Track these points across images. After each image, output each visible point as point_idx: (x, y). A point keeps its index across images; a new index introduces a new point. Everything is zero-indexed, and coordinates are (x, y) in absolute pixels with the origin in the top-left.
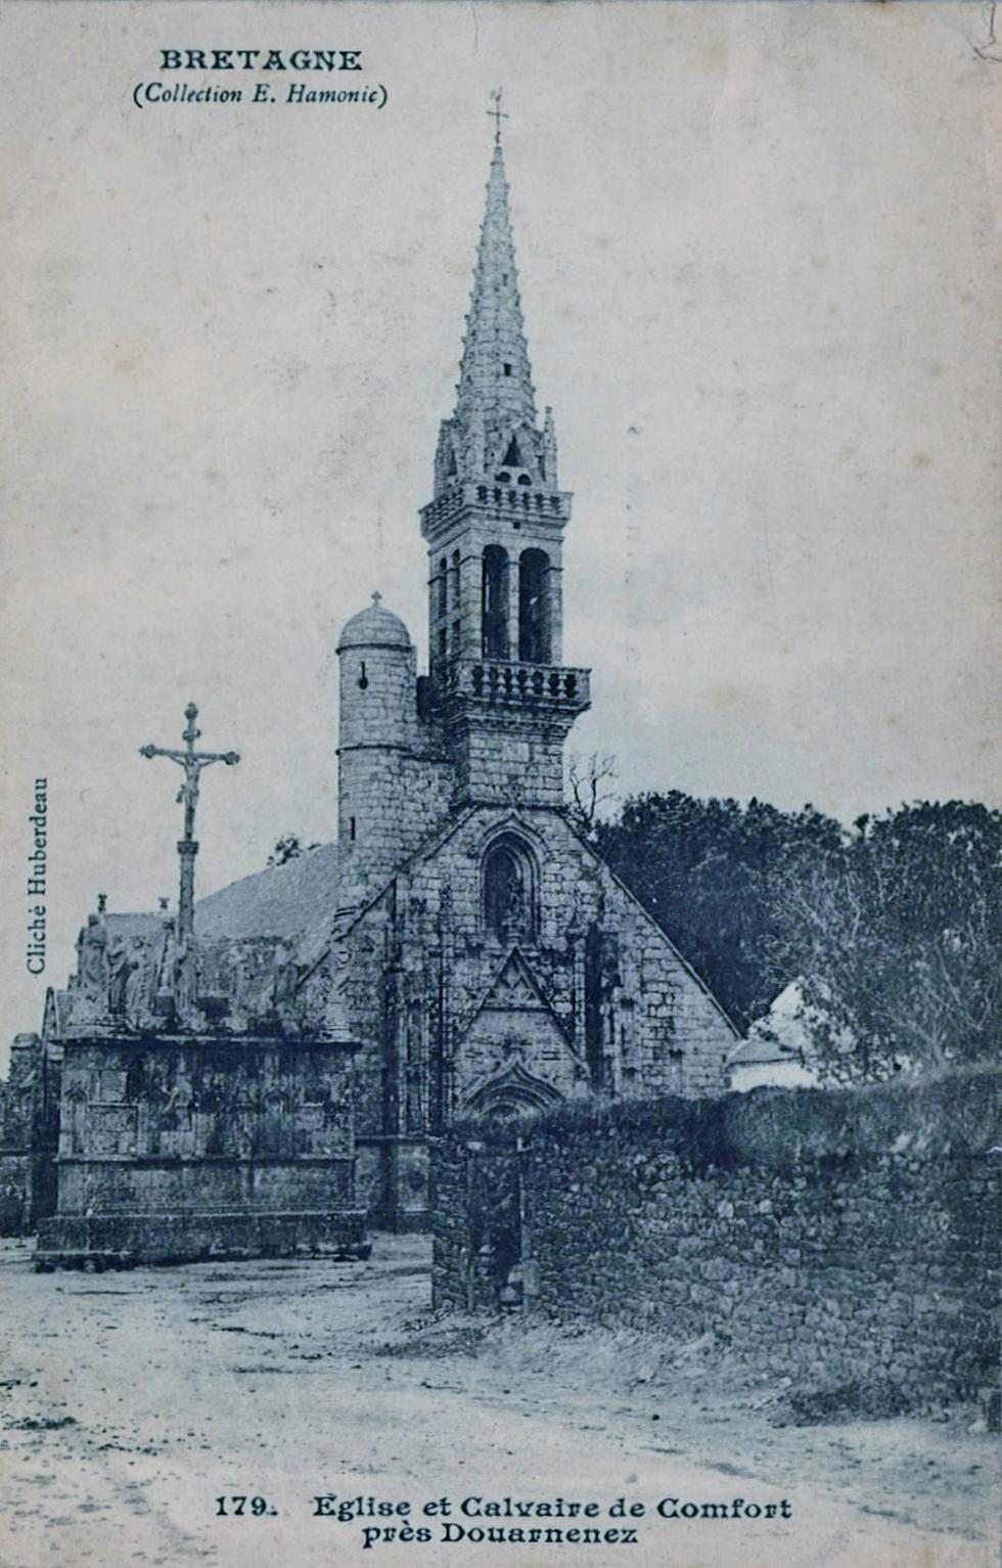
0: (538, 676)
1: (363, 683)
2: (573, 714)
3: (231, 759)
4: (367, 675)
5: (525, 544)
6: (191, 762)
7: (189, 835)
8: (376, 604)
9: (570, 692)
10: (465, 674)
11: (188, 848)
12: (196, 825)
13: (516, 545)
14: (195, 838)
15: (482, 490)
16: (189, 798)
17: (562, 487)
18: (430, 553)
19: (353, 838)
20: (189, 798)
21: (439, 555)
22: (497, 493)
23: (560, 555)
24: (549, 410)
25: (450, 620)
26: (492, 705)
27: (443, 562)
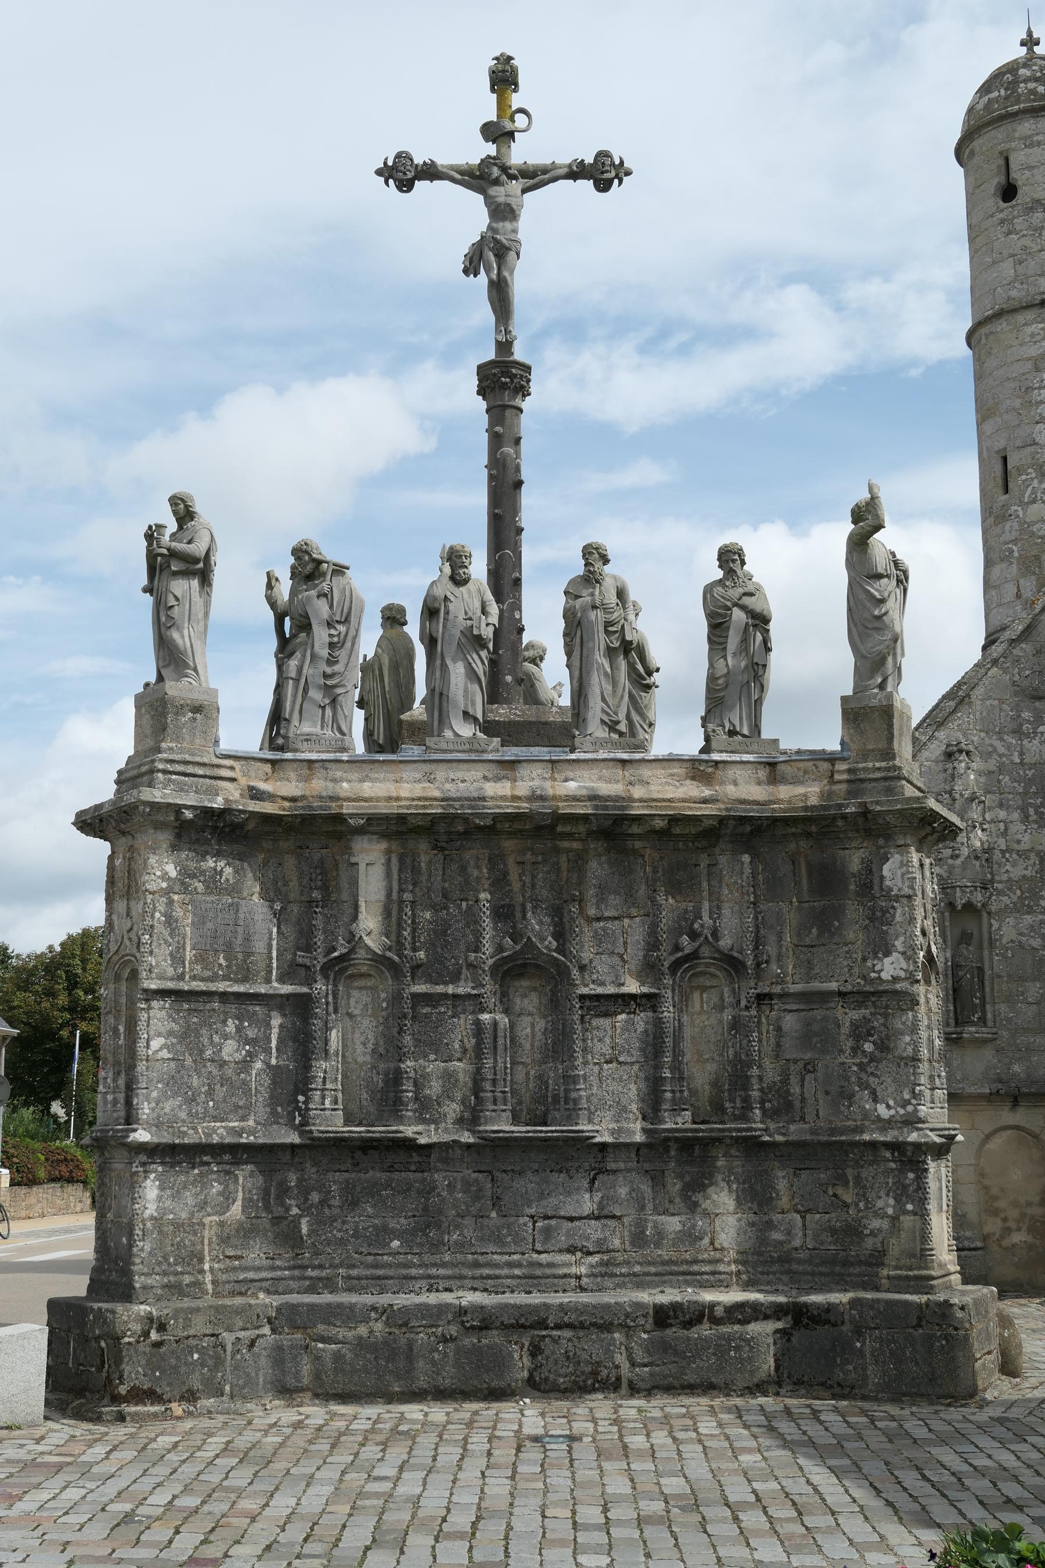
1: (1009, 192)
4: (1013, 175)
8: (1030, 50)
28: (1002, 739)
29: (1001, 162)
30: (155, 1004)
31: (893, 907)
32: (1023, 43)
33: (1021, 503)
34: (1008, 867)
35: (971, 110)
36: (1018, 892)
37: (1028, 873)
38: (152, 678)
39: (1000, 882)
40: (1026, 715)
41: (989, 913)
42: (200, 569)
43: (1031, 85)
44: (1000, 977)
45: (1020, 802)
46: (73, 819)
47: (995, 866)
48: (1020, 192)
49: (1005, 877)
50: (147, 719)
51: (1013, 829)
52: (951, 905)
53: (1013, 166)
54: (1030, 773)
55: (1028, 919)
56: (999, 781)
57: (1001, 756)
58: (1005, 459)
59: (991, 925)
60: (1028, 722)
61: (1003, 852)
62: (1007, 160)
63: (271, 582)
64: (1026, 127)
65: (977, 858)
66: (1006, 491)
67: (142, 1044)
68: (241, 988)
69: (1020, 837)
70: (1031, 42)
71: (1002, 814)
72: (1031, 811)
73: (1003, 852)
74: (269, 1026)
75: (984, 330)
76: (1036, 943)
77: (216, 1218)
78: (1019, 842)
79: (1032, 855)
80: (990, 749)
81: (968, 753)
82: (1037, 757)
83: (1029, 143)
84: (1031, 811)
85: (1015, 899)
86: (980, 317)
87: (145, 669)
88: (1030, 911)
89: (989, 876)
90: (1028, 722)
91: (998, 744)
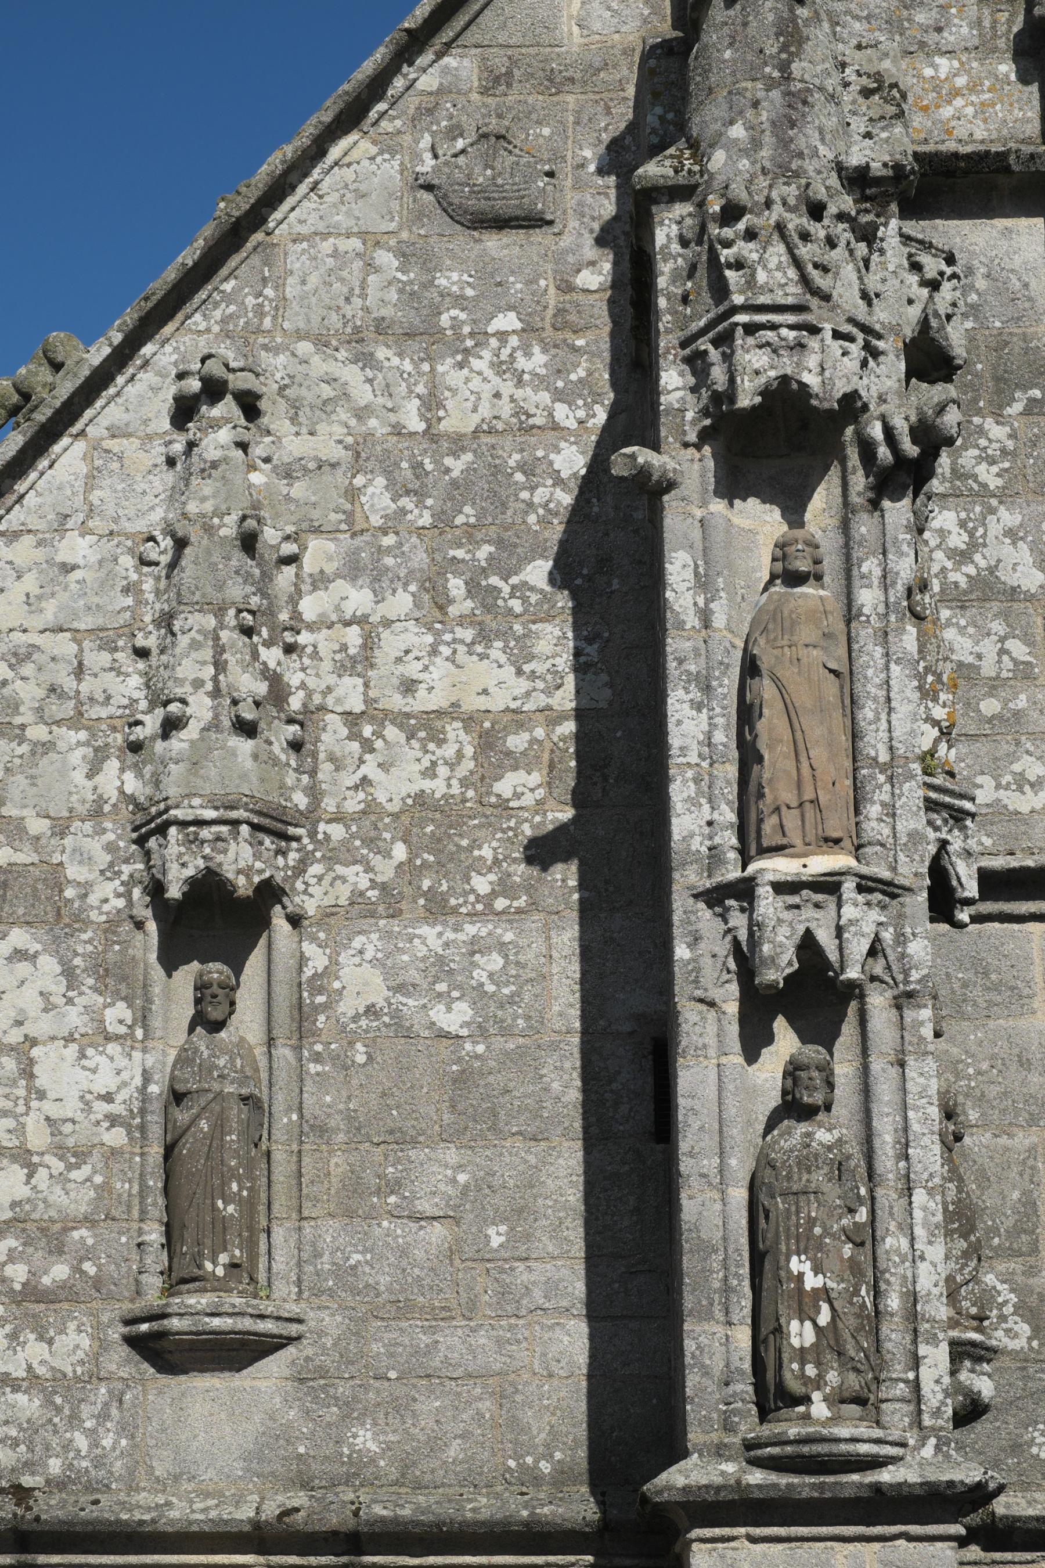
28: (366, 360)
34: (370, 769)
36: (400, 852)
37: (437, 787)
39: (337, 818)
40: (450, 279)
41: (295, 921)
44: (322, 1130)
45: (420, 558)
47: (326, 769)
49: (353, 804)
51: (391, 644)
52: (156, 889)
54: (457, 466)
55: (431, 937)
56: (352, 494)
57: (362, 413)
59: (302, 960)
60: (459, 302)
61: (352, 719)
65: (247, 729)
69: (412, 669)
71: (358, 599)
72: (456, 586)
73: (352, 719)
76: (454, 1017)
78: (409, 687)
79: (454, 730)
80: (327, 391)
81: (250, 406)
82: (485, 411)
84: (456, 586)
85: (385, 871)
88: (438, 909)
89: (301, 800)
90: (459, 302)
91: (352, 375)
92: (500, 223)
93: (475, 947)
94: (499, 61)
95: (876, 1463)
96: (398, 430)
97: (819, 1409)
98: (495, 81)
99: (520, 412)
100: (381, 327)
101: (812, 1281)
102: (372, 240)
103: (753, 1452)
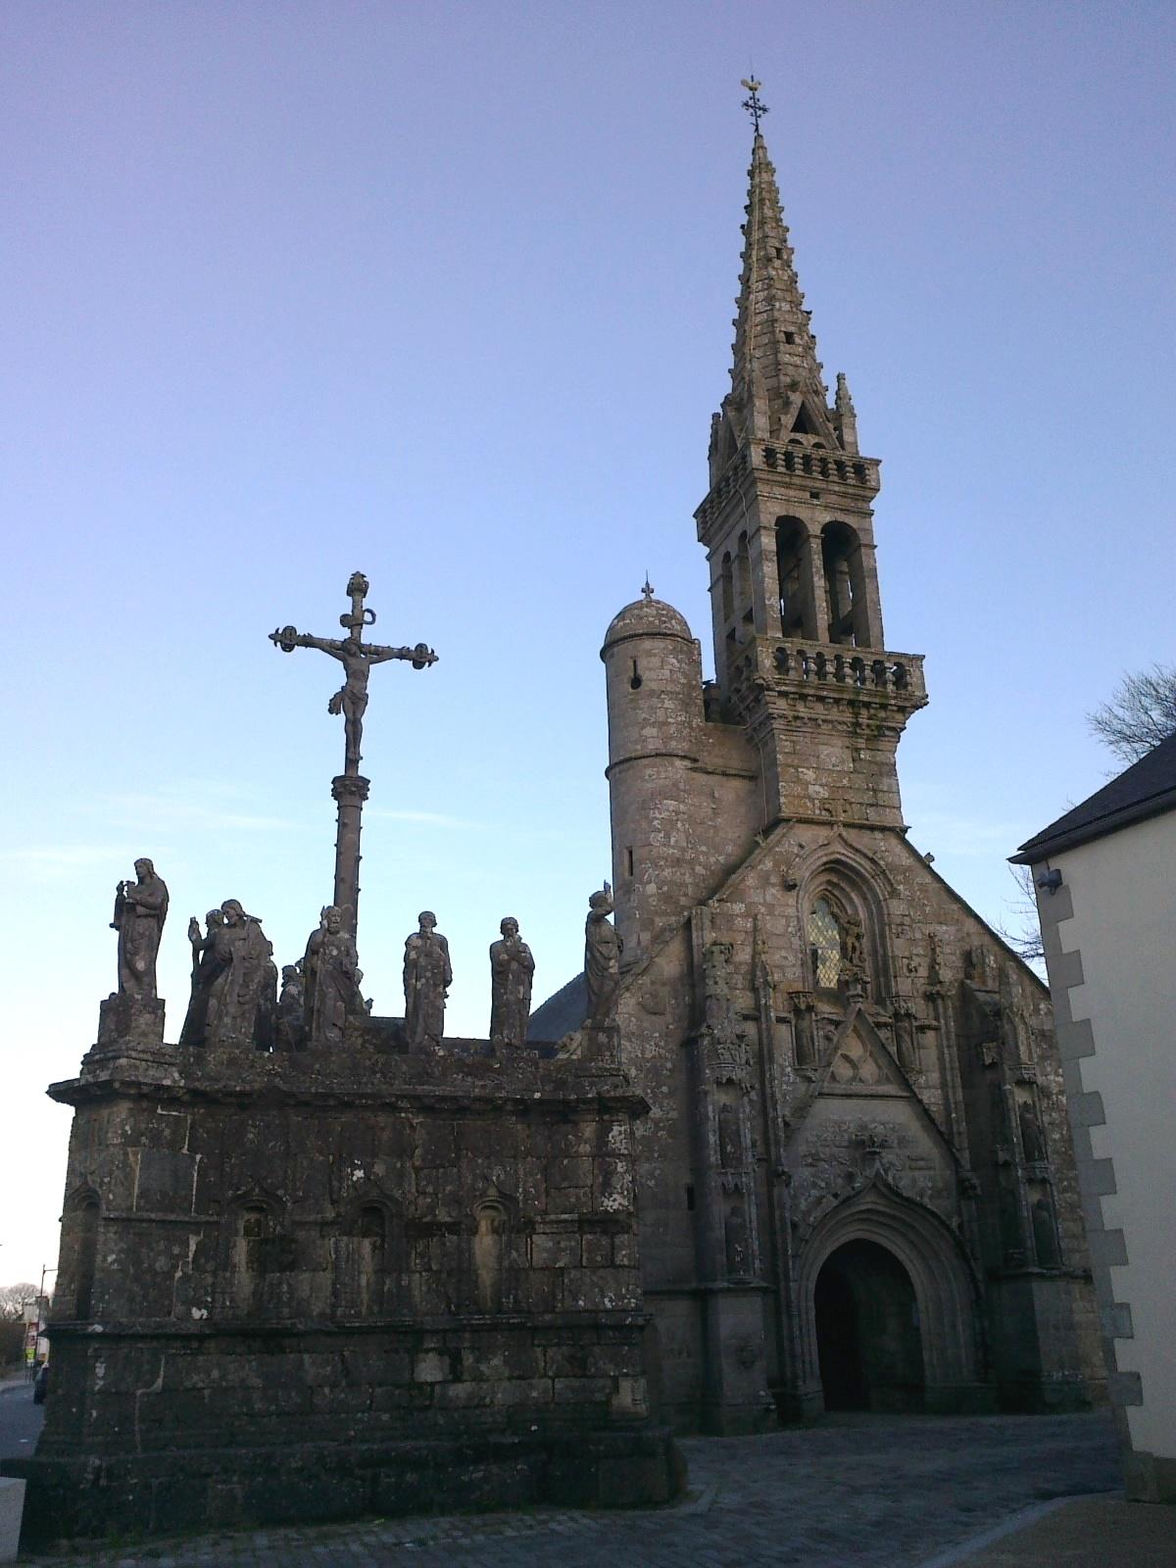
0: (857, 664)
2: (904, 712)
3: (420, 657)
4: (640, 672)
5: (827, 517)
6: (356, 656)
7: (352, 760)
8: (648, 596)
9: (901, 679)
10: (766, 661)
11: (350, 790)
12: (365, 747)
13: (816, 519)
14: (363, 770)
15: (770, 454)
16: (350, 703)
17: (865, 451)
18: (708, 558)
19: (632, 874)
20: (350, 703)
21: (722, 551)
22: (789, 457)
23: (869, 531)
24: (840, 378)
25: (739, 614)
26: (803, 697)
27: (727, 555)
29: (631, 664)
30: (110, 1228)
31: (616, 1163)
32: (643, 591)
33: (641, 883)
35: (611, 629)
38: (116, 990)
40: (646, 1025)
42: (157, 912)
43: (651, 619)
46: (47, 1089)
48: (643, 684)
50: (112, 1018)
53: (639, 668)
57: (630, 1052)
58: (631, 853)
62: (635, 662)
63: (194, 923)
64: (647, 644)
66: (632, 874)
67: (99, 1258)
68: (172, 1217)
70: (647, 590)
74: (188, 1246)
75: (617, 770)
76: (652, 1183)
77: (144, 1390)
83: (649, 653)
86: (616, 760)
87: (107, 982)
88: (648, 1159)
92: (655, 1014)
93: (655, 1168)
94: (653, 978)
95: (750, 1283)
96: (637, 1056)
97: (742, 1273)
98: (653, 983)
99: (659, 1054)
100: (633, 1034)
101: (739, 1249)
102: (631, 1015)
103: (728, 1281)
